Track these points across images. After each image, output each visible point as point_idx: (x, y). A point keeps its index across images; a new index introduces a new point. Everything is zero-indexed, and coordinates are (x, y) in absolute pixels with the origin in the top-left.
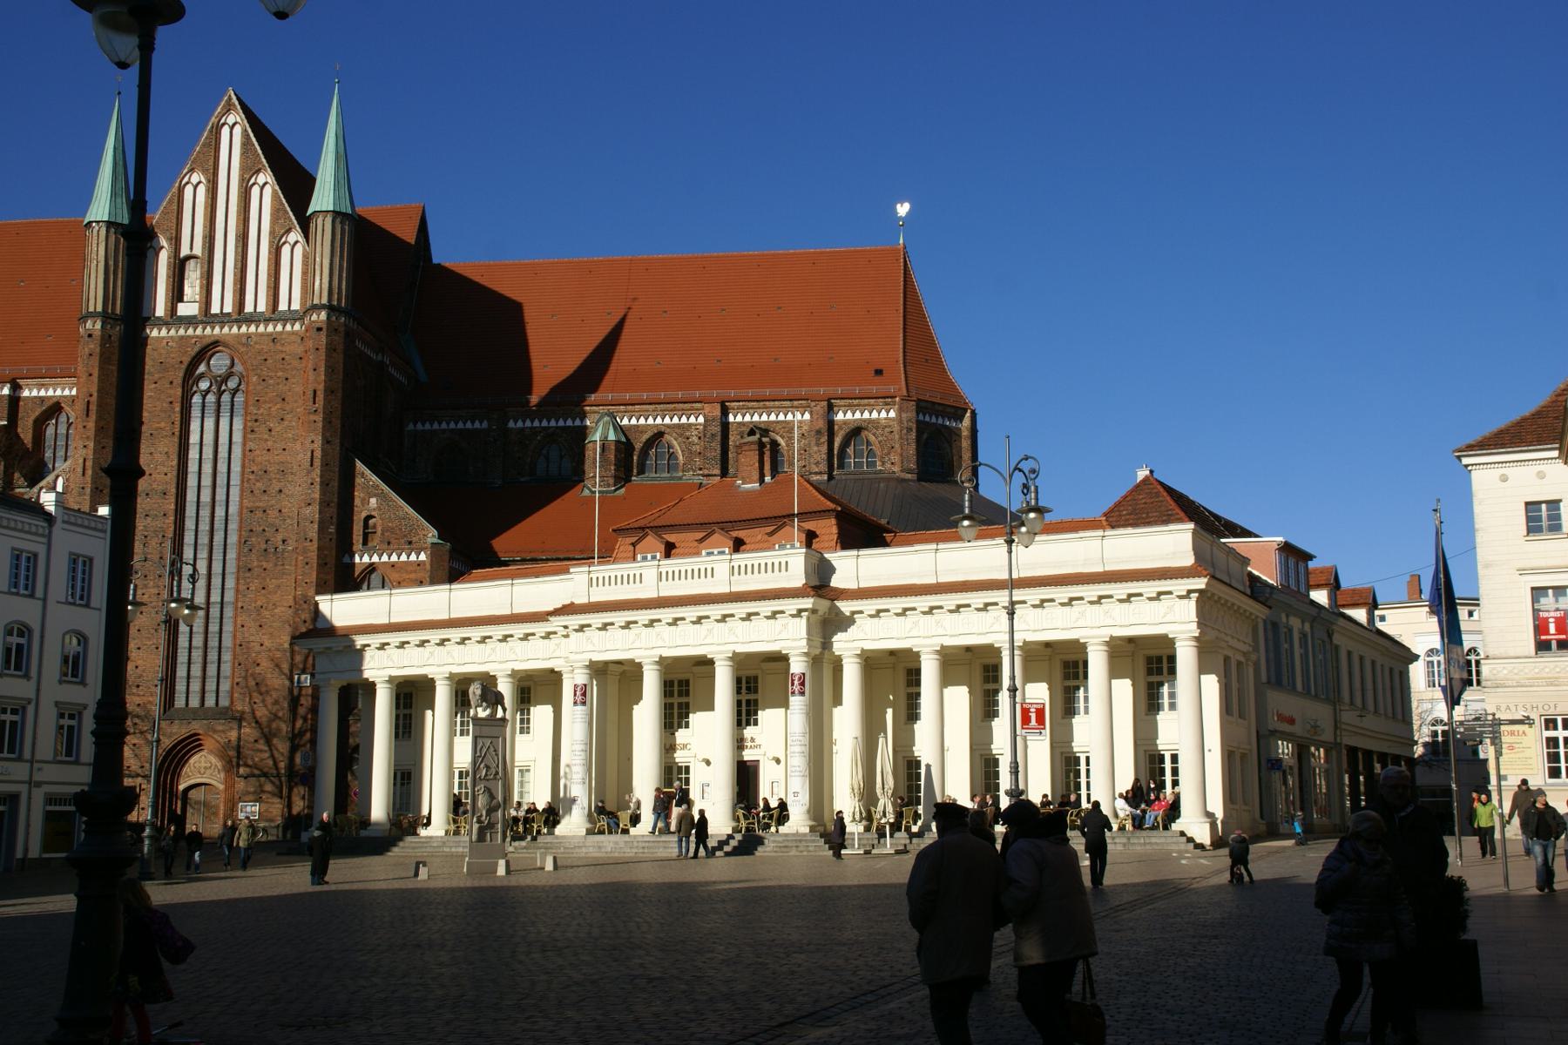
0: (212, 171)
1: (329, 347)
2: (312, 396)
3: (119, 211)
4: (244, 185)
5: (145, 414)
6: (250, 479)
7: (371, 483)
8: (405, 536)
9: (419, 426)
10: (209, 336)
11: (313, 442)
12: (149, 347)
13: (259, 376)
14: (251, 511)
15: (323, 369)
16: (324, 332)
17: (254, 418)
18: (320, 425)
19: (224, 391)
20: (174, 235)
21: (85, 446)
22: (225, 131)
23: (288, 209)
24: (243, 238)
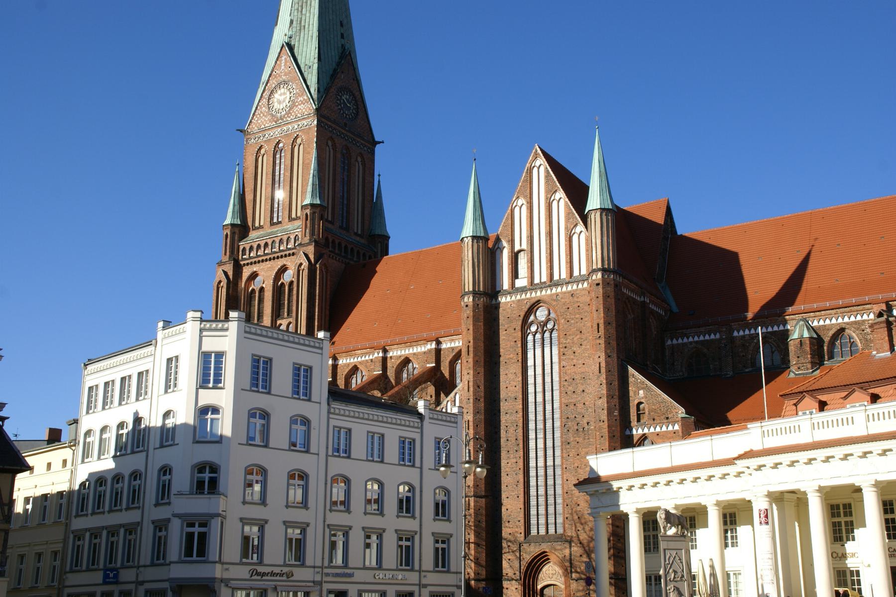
0: (529, 196)
1: (605, 295)
2: (597, 327)
3: (478, 229)
4: (548, 201)
5: (501, 350)
6: (564, 385)
7: (639, 381)
8: (664, 414)
9: (675, 342)
10: (534, 297)
11: (599, 357)
12: (501, 309)
13: (565, 319)
14: (567, 406)
15: (602, 310)
16: (601, 286)
17: (564, 346)
18: (603, 346)
19: (546, 331)
20: (510, 239)
21: (468, 374)
22: (535, 171)
23: (575, 212)
24: (550, 234)
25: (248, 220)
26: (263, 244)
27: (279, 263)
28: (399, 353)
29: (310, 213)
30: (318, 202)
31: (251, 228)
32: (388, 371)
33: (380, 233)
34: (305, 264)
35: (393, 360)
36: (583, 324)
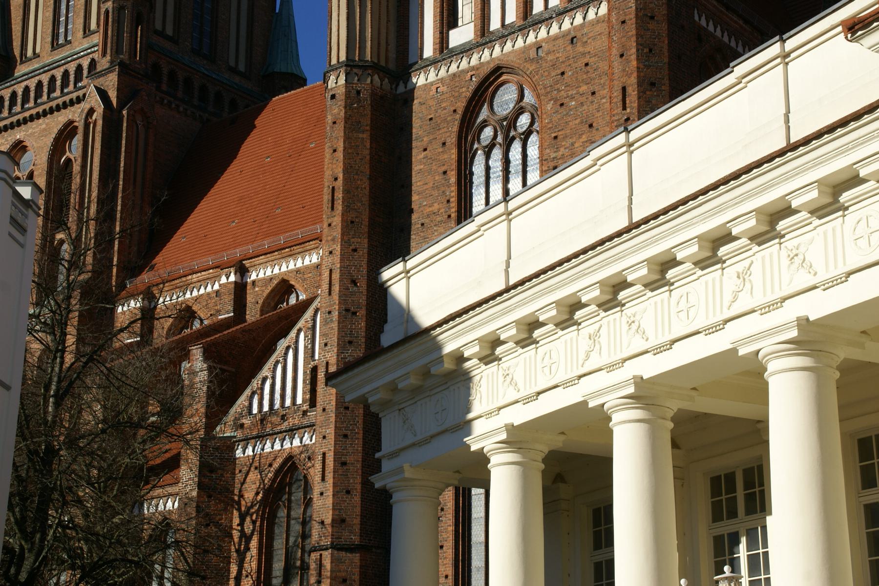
1: (641, 14)
2: (620, 97)
5: (415, 197)
10: (488, 62)
12: (415, 102)
13: (556, 100)
15: (634, 50)
19: (513, 138)
25: (15, 44)
26: (35, 85)
27: (61, 118)
28: (269, 273)
29: (113, 8)
31: (18, 59)
32: (247, 313)
33: (284, 70)
34: (100, 108)
35: (257, 289)
36: (595, 106)
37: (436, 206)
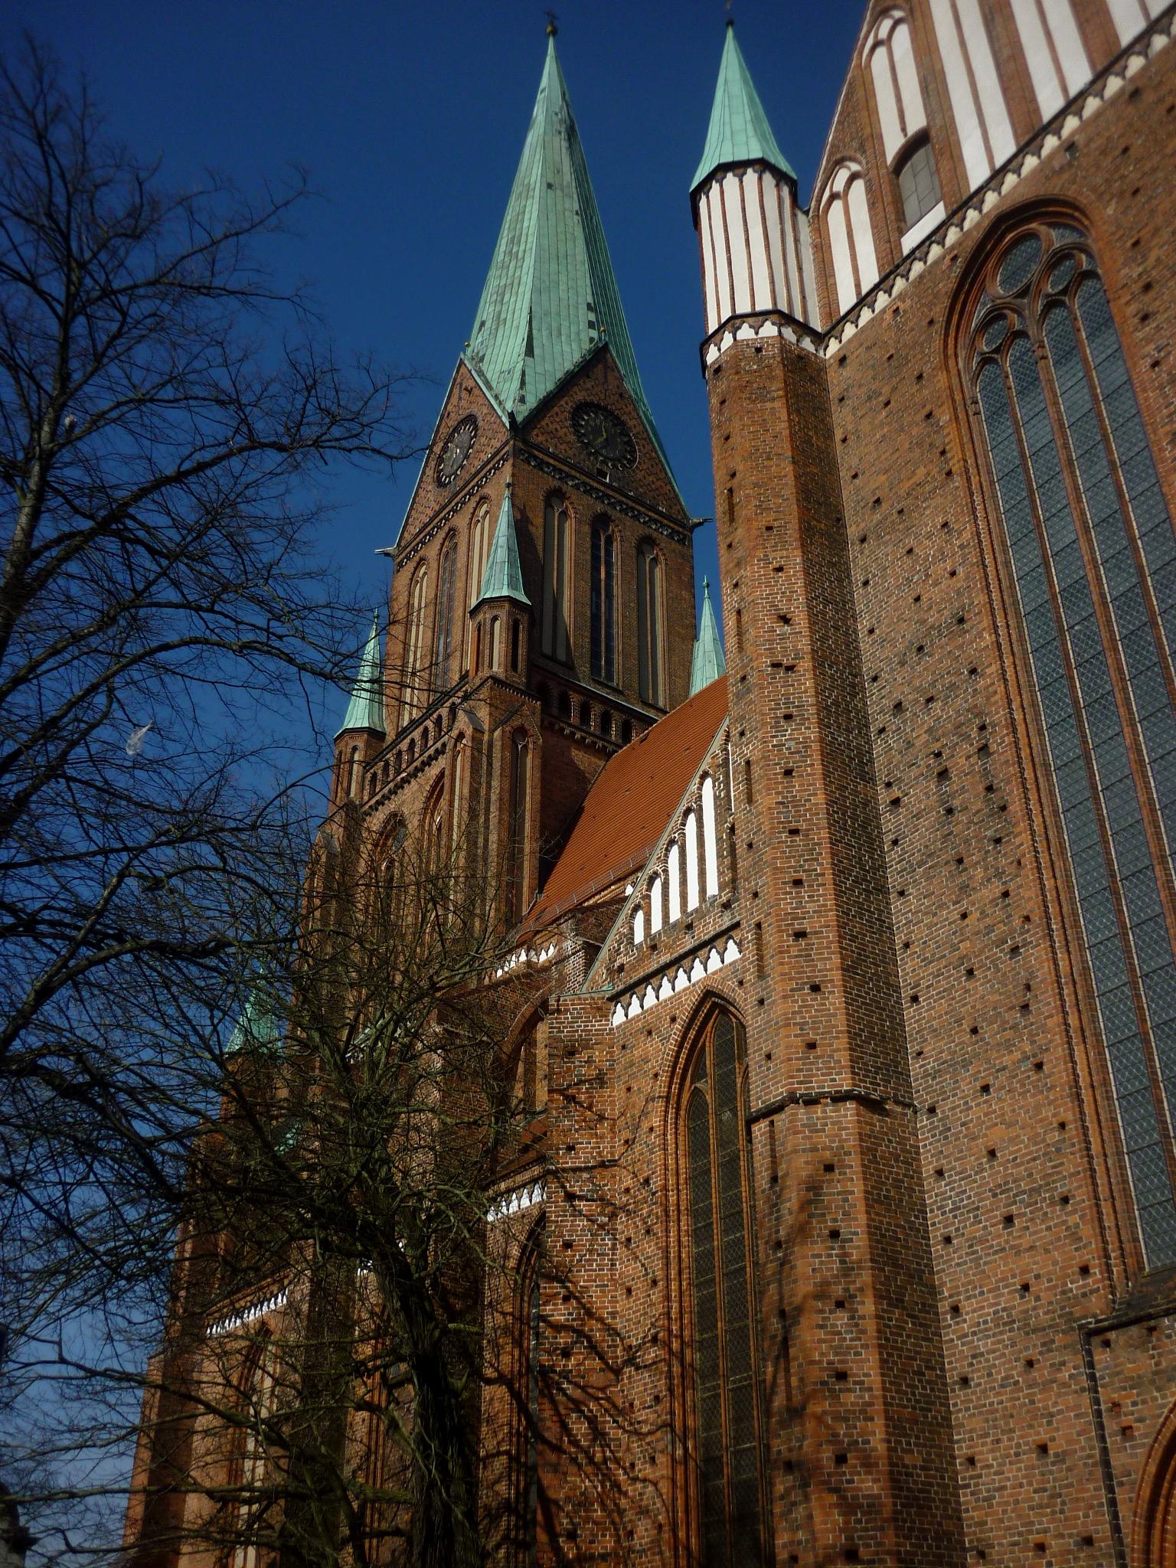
13: (1121, 194)
30: (505, 592)
37: (921, 472)
